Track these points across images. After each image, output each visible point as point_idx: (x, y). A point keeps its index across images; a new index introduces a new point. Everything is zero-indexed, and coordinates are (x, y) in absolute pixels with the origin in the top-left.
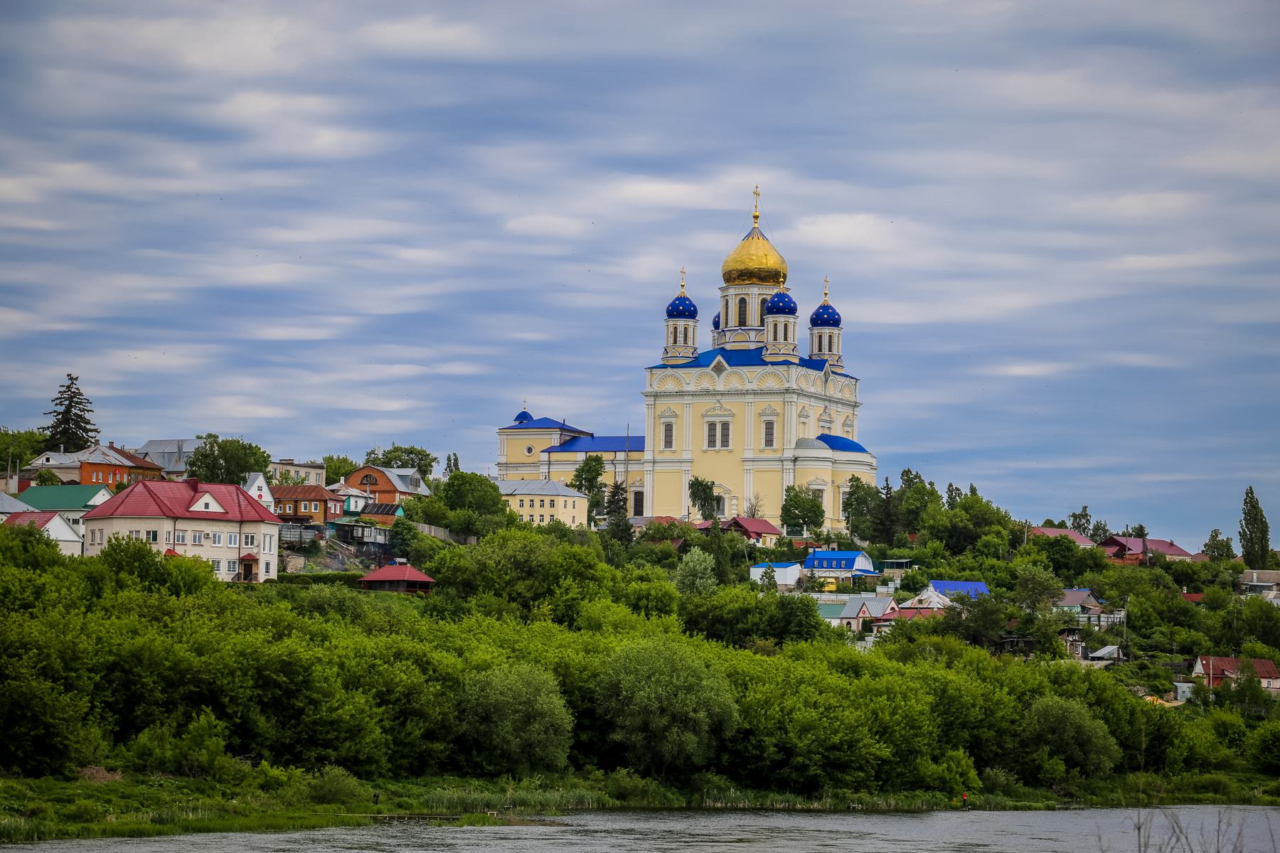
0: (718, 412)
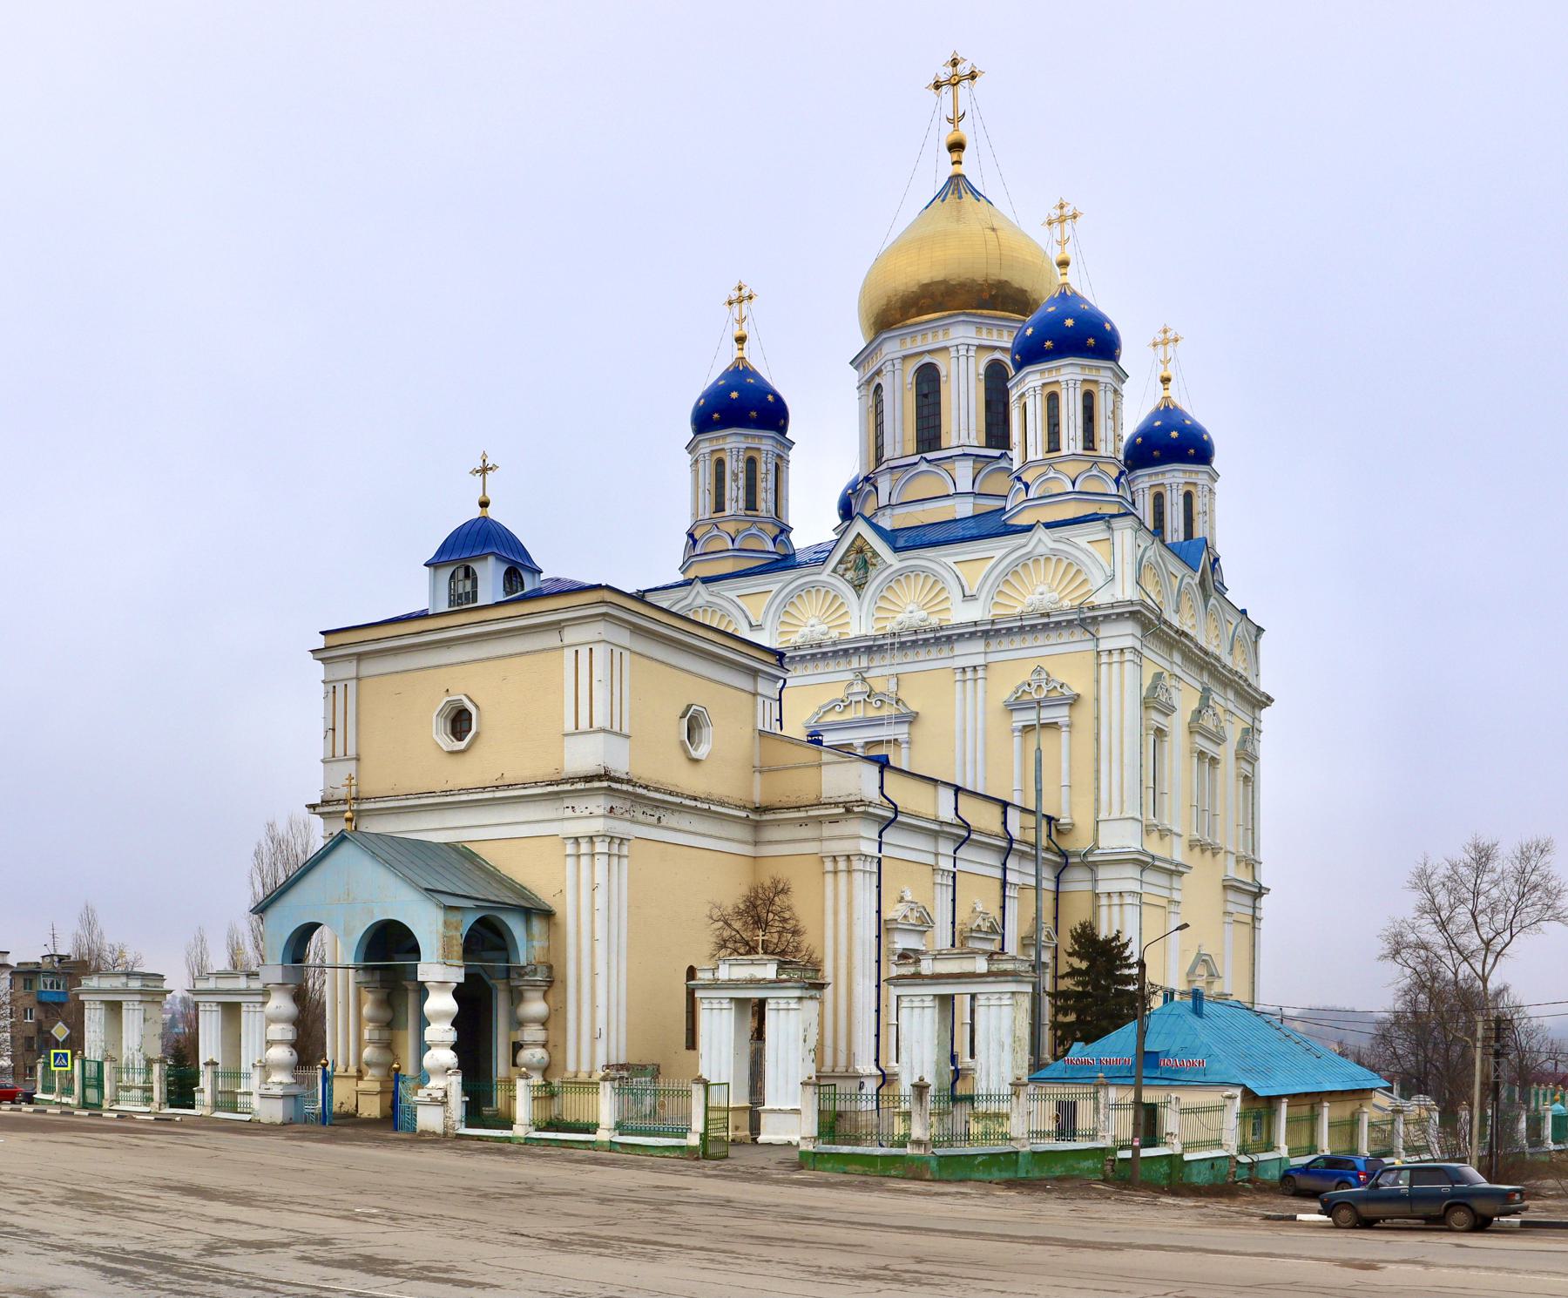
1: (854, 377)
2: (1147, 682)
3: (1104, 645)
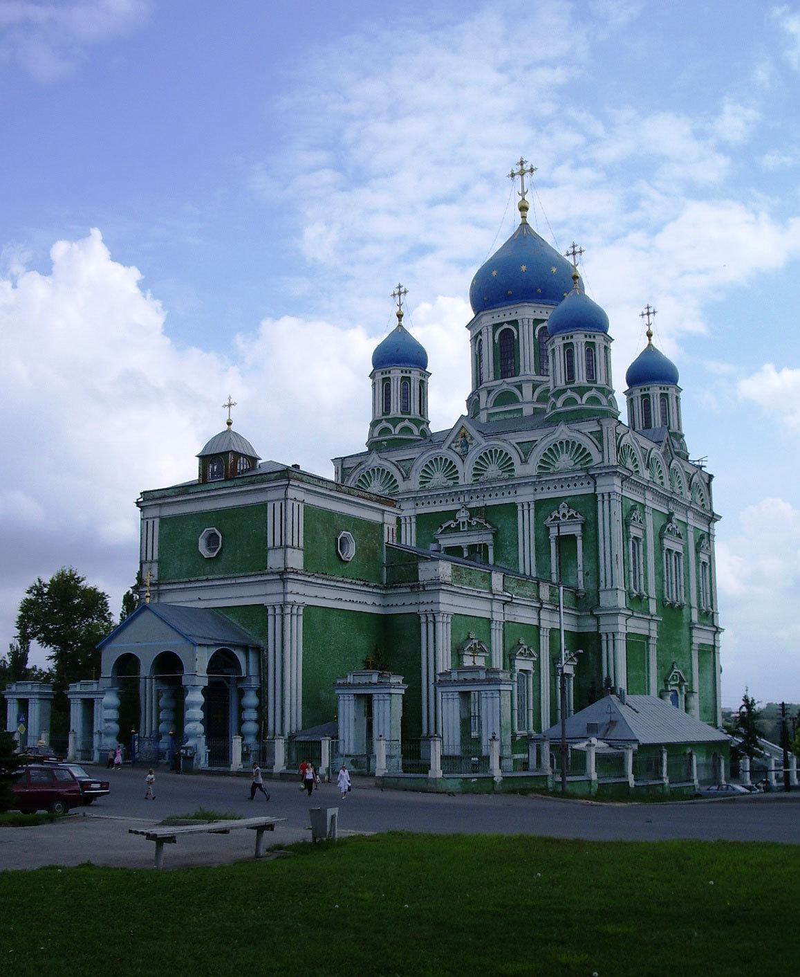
1: (467, 334)
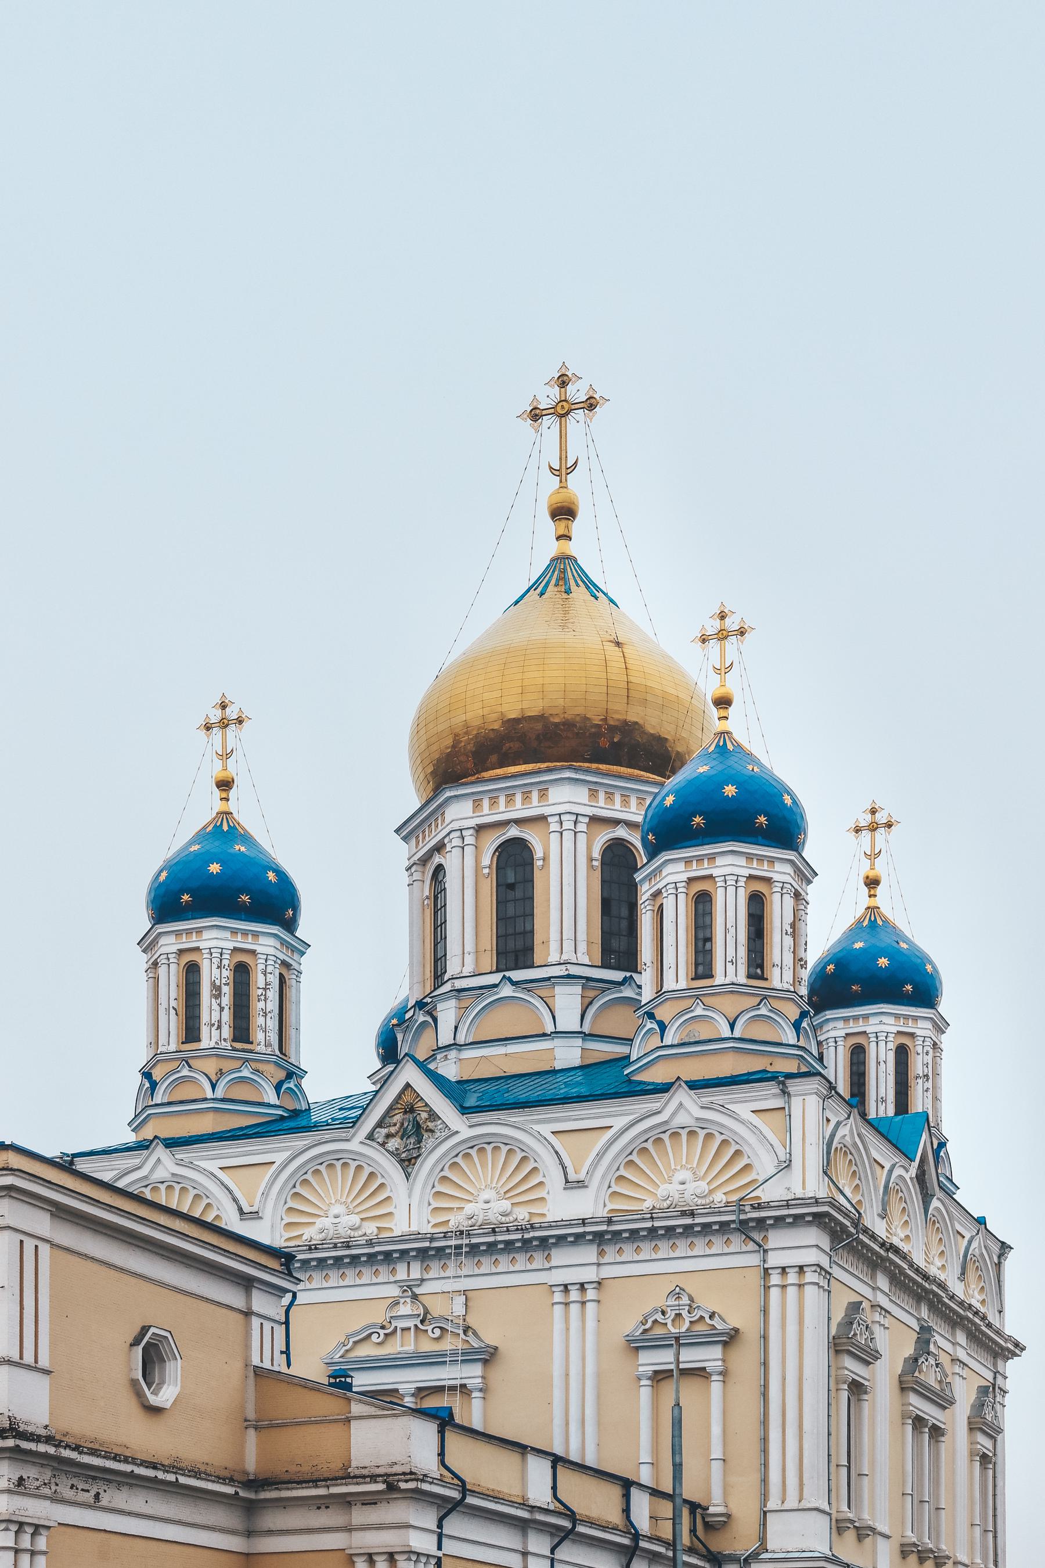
0: (402, 1346)
1: (402, 852)
2: (838, 1316)
3: (775, 1260)
